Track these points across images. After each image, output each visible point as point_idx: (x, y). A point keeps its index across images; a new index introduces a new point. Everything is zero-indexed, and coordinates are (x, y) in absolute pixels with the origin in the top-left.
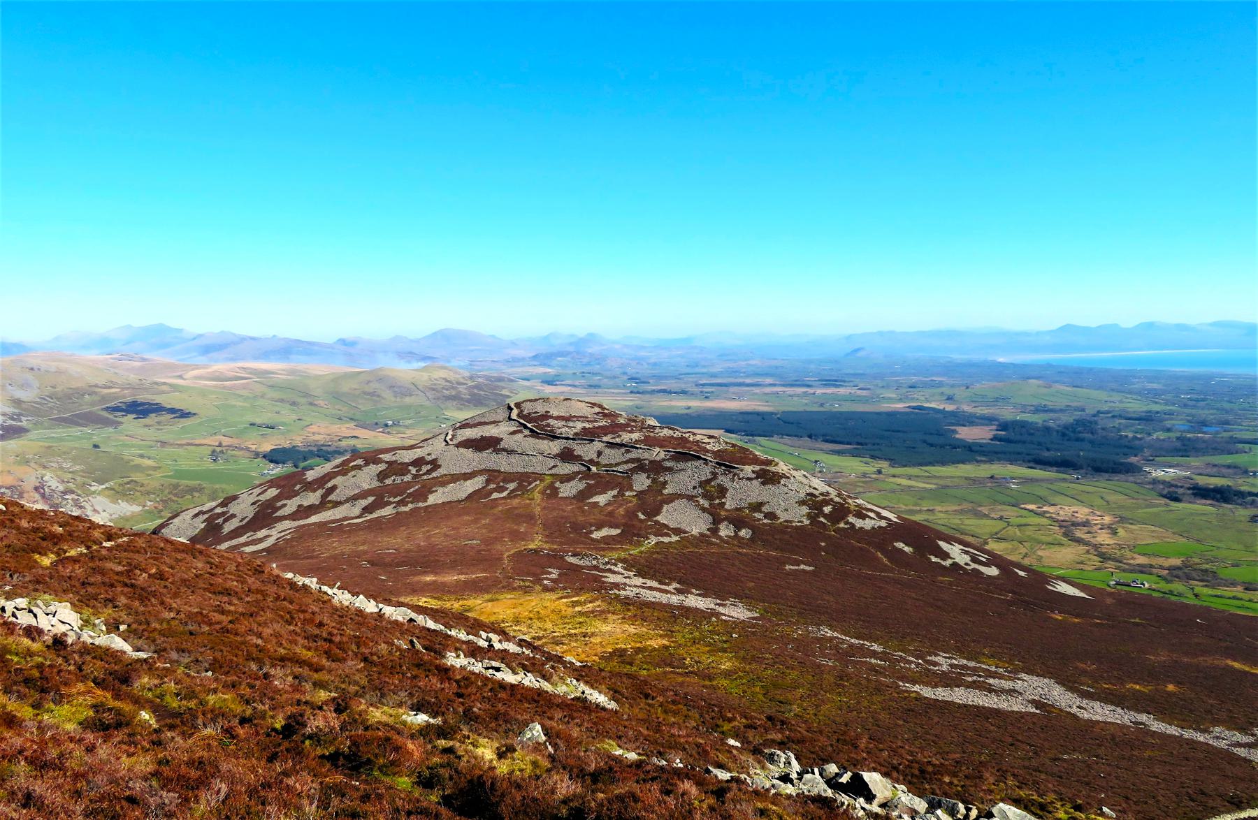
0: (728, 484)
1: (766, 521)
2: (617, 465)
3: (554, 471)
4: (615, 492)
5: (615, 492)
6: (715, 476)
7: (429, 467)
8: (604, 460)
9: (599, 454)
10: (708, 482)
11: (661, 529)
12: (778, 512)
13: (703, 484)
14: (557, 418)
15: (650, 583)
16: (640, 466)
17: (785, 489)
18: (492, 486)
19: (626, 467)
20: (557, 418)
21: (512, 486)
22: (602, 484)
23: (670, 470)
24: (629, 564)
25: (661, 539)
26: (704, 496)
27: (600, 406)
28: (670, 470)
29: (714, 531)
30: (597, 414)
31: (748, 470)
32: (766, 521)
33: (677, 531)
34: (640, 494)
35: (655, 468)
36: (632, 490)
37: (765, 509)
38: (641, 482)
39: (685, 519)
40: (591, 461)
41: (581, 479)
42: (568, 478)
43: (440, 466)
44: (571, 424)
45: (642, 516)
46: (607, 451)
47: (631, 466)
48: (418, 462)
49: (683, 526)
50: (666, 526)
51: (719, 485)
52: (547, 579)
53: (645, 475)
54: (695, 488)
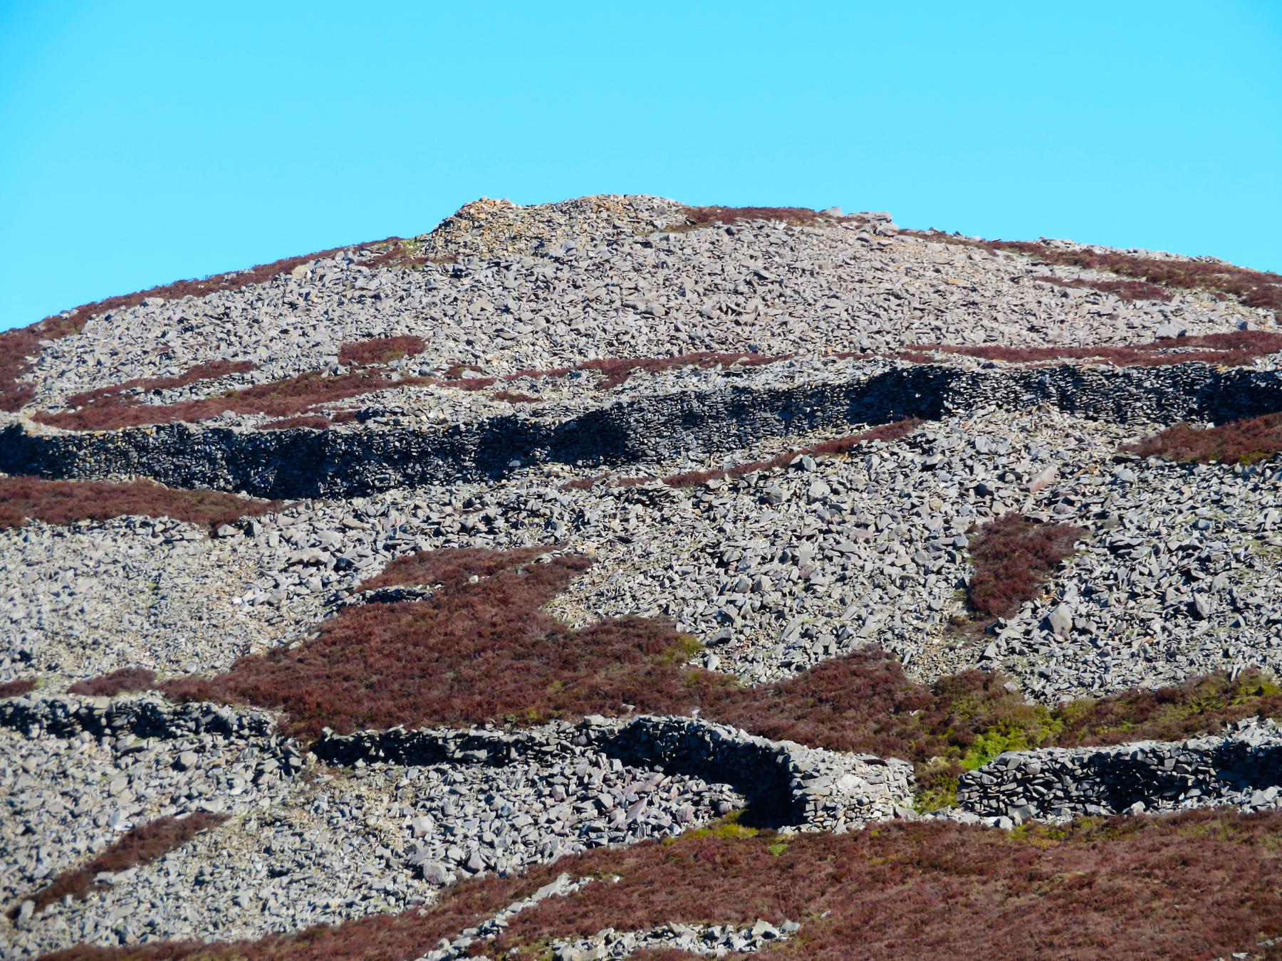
9: (1009, 566)
40: (853, 696)
46: (1165, 508)
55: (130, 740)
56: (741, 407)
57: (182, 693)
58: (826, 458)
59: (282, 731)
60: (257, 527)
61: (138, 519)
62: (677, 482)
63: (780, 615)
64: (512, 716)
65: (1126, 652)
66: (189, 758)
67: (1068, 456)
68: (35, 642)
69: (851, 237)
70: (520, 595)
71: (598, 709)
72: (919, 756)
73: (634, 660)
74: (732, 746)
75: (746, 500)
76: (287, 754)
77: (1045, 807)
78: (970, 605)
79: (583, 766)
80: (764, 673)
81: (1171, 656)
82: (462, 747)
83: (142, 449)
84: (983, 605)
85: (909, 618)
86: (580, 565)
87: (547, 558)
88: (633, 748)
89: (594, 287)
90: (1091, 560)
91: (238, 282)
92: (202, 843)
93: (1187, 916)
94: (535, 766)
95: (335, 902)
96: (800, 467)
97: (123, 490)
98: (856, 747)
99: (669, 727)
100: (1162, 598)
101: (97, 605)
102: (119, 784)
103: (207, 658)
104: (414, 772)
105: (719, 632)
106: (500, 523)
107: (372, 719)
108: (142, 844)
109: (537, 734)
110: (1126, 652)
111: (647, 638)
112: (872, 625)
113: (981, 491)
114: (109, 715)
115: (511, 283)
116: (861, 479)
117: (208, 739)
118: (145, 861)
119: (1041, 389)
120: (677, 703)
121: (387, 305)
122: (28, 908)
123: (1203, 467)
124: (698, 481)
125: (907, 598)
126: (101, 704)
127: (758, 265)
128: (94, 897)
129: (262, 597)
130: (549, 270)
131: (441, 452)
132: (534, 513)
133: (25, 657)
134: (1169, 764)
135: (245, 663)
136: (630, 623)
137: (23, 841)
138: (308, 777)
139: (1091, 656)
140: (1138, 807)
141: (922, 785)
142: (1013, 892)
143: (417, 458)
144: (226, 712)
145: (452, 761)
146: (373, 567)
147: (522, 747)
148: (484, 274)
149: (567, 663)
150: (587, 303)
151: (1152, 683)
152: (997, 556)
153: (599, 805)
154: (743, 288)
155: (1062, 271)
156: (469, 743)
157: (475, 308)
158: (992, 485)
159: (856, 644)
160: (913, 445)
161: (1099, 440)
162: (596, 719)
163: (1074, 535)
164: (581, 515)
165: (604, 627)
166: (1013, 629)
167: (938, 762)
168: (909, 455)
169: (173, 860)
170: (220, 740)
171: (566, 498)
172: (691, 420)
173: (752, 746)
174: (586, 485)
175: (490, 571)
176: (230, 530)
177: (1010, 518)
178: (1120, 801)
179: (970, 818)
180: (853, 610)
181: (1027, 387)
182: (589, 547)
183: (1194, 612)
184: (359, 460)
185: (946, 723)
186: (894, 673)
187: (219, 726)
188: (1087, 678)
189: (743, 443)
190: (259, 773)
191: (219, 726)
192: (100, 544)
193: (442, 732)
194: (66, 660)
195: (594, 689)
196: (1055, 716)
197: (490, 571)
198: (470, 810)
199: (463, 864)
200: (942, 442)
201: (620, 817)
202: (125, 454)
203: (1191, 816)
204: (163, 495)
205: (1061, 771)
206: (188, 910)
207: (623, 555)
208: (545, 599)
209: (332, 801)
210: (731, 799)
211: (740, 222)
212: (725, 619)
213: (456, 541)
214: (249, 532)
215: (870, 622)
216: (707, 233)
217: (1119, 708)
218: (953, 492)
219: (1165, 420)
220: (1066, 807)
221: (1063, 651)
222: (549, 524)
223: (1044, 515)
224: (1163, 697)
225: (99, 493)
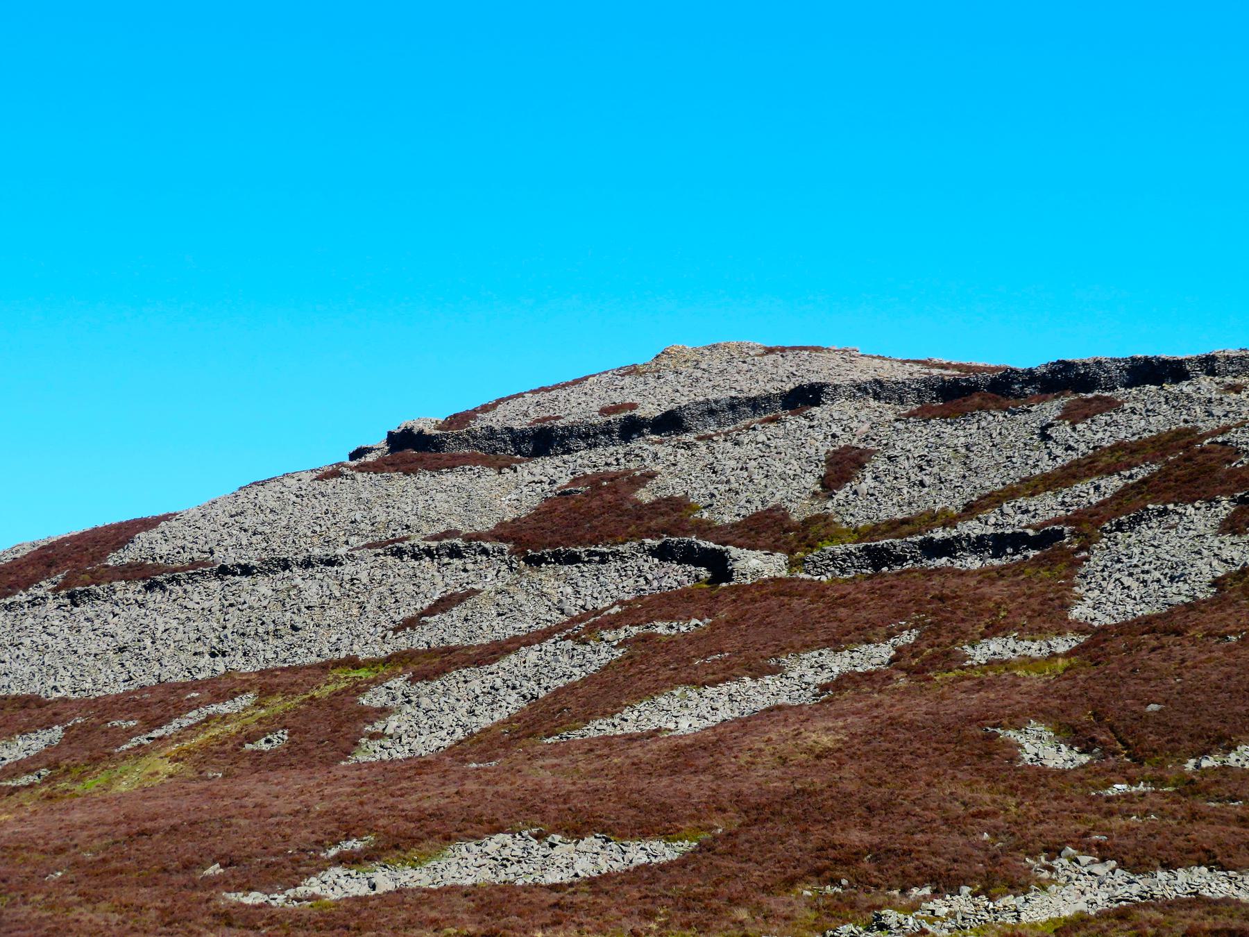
2: (970, 510)
9: (843, 467)
19: (1048, 507)
40: (766, 528)
45: (1039, 747)
46: (915, 439)
55: (446, 560)
56: (733, 405)
57: (468, 538)
58: (766, 425)
59: (511, 553)
60: (519, 469)
61: (467, 467)
62: (700, 439)
63: (737, 493)
64: (610, 541)
65: (890, 503)
66: (470, 567)
67: (875, 419)
68: (413, 520)
69: (838, 358)
70: (623, 489)
71: (651, 537)
72: (791, 552)
73: (669, 515)
74: (706, 549)
75: (729, 444)
76: (512, 562)
77: (843, 571)
78: (823, 486)
79: (641, 562)
80: (727, 519)
81: (910, 504)
82: (588, 556)
83: (474, 438)
84: (829, 485)
85: (795, 494)
86: (652, 476)
87: (638, 473)
88: (663, 553)
89: (718, 380)
90: (878, 464)
91: (564, 386)
92: (469, 603)
93: (883, 607)
94: (619, 563)
95: (524, 626)
96: (754, 429)
97: (465, 456)
98: (761, 549)
99: (679, 543)
100: (909, 479)
101: (442, 502)
102: (438, 579)
103: (485, 523)
104: (566, 568)
105: (709, 502)
106: (623, 461)
107: (550, 545)
108: (444, 605)
109: (620, 549)
110: (890, 503)
111: (677, 506)
112: (778, 496)
113: (834, 436)
114: (437, 549)
115: (681, 380)
116: (782, 432)
117: (479, 558)
118: (443, 611)
119: (865, 390)
120: (687, 533)
121: (626, 391)
122: (391, 633)
123: (933, 421)
124: (710, 438)
125: (795, 483)
126: (434, 544)
127: (793, 370)
128: (419, 628)
129: (514, 497)
130: (699, 373)
131: (603, 433)
132: (637, 456)
133: (408, 527)
134: (899, 549)
135: (502, 525)
136: (670, 499)
137: (393, 606)
138: (520, 572)
139: (875, 506)
140: (885, 569)
141: (792, 565)
142: (812, 602)
143: (589, 436)
144: (487, 545)
145: (583, 562)
146: (565, 481)
147: (614, 554)
148: (671, 377)
149: (640, 518)
150: (714, 387)
151: (899, 516)
152: (837, 463)
153: (646, 579)
154: (785, 379)
156: (591, 554)
157: (663, 391)
158: (838, 434)
159: (770, 505)
160: (806, 417)
161: (890, 412)
162: (648, 541)
163: (872, 453)
164: (656, 454)
165: (659, 501)
166: (840, 495)
167: (799, 554)
168: (803, 422)
169: (455, 611)
170: (484, 558)
171: (652, 448)
172: (712, 412)
173: (714, 549)
174: (661, 443)
175: (612, 480)
176: (507, 470)
177: (846, 447)
178: (877, 568)
179: (808, 577)
180: (770, 489)
181: (859, 390)
182: (658, 468)
183: (922, 484)
184: (567, 438)
185: (806, 537)
186: (786, 516)
187: (485, 552)
188: (871, 515)
189: (734, 421)
190: (499, 571)
191: (485, 552)
192: (449, 478)
193: (580, 549)
194: (425, 528)
195: (649, 528)
196: (854, 532)
197: (612, 480)
198: (589, 583)
199: (583, 607)
200: (819, 415)
201: (655, 584)
202: (467, 440)
203: (908, 571)
204: (482, 457)
205: (850, 554)
206: (459, 632)
207: (671, 469)
208: (635, 490)
209: (529, 582)
210: (704, 573)
211: (788, 352)
212: (713, 495)
213: (602, 469)
214: (515, 471)
215: (778, 495)
216: (772, 357)
217: (883, 528)
218: (821, 437)
219: (921, 402)
220: (852, 571)
221: (860, 504)
222: (643, 459)
223: (861, 446)
224: (904, 522)
225: (454, 457)
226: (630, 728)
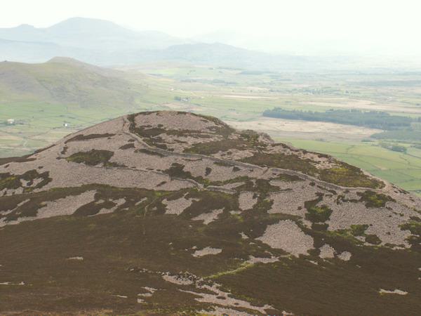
0: (333, 207)
1: (367, 244)
3: (163, 188)
4: (221, 211)
5: (221, 211)
6: (320, 196)
7: (40, 180)
8: (212, 178)
9: (208, 171)
10: (314, 202)
11: (264, 250)
12: (381, 237)
13: (309, 205)
14: (171, 132)
15: (243, 304)
16: (248, 185)
17: (389, 212)
18: (101, 201)
20: (171, 132)
21: (122, 201)
22: (207, 203)
23: (277, 189)
24: (225, 283)
25: (259, 260)
26: (308, 217)
27: (214, 120)
28: (277, 189)
29: (315, 253)
30: (210, 128)
31: (354, 192)
32: (367, 244)
33: (278, 252)
34: (246, 214)
35: (263, 188)
36: (237, 208)
37: (368, 232)
38: (247, 201)
39: (288, 239)
40: (199, 179)
41: (187, 198)
42: (175, 196)
43: (50, 180)
44: (182, 139)
45: (245, 237)
47: (239, 184)
48: (31, 175)
49: (285, 247)
50: (268, 247)
51: (324, 207)
52: (141, 298)
53: (251, 195)
54: (300, 208)
80: (195, 176)
108: (163, 183)
111: (188, 173)
155: (201, 118)
226: (199, 219)
